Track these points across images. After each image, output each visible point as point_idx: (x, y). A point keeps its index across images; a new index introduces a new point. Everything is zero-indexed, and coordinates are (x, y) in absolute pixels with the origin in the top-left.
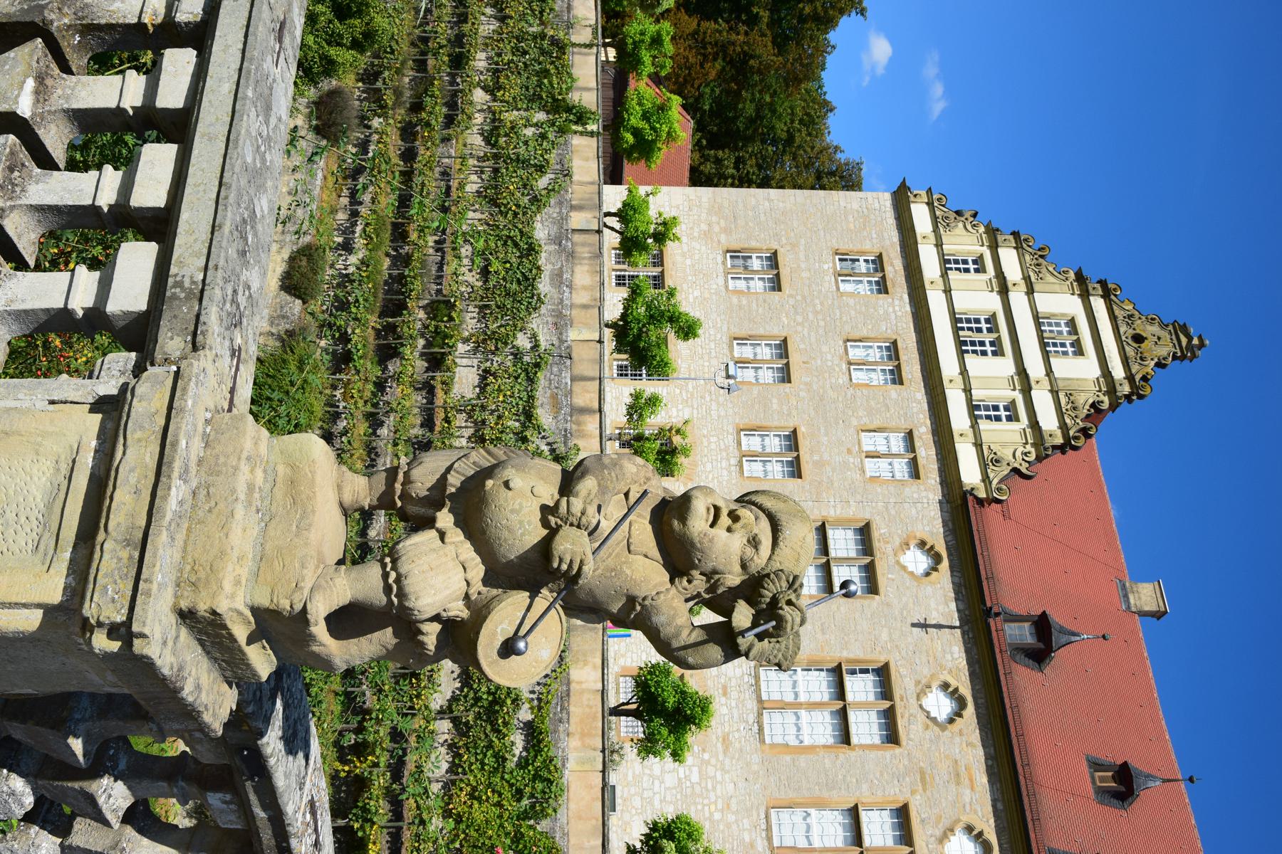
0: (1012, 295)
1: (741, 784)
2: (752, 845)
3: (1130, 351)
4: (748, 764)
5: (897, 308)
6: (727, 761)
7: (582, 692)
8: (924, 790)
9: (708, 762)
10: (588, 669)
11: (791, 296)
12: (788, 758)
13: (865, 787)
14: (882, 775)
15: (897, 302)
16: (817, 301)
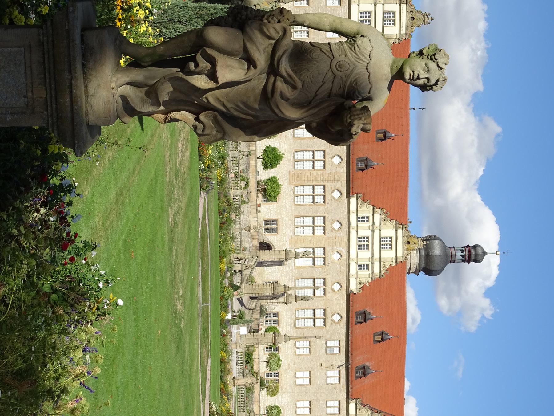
0: (378, 5)
1: (288, 146)
2: (290, 160)
3: (409, 23)
4: (291, 142)
5: (342, 11)
6: (286, 141)
7: (252, 165)
8: (330, 147)
9: (281, 142)
10: (253, 161)
11: (312, 8)
12: (299, 140)
13: (316, 147)
14: (320, 144)
15: (343, 9)
16: (319, 9)
